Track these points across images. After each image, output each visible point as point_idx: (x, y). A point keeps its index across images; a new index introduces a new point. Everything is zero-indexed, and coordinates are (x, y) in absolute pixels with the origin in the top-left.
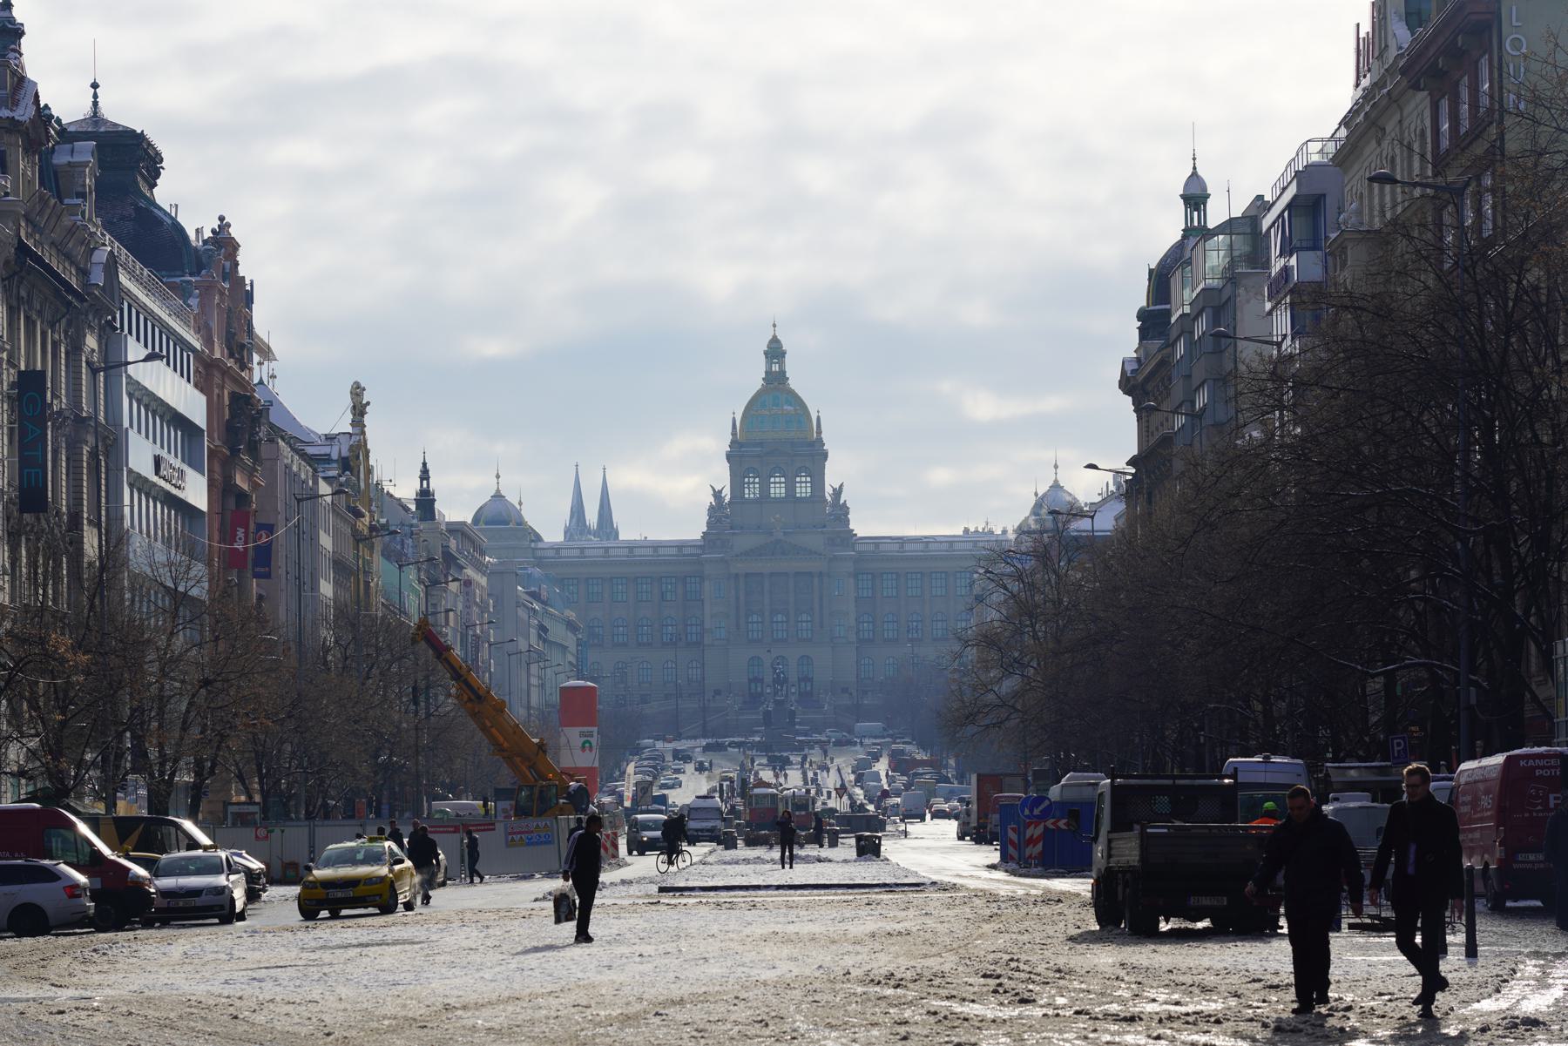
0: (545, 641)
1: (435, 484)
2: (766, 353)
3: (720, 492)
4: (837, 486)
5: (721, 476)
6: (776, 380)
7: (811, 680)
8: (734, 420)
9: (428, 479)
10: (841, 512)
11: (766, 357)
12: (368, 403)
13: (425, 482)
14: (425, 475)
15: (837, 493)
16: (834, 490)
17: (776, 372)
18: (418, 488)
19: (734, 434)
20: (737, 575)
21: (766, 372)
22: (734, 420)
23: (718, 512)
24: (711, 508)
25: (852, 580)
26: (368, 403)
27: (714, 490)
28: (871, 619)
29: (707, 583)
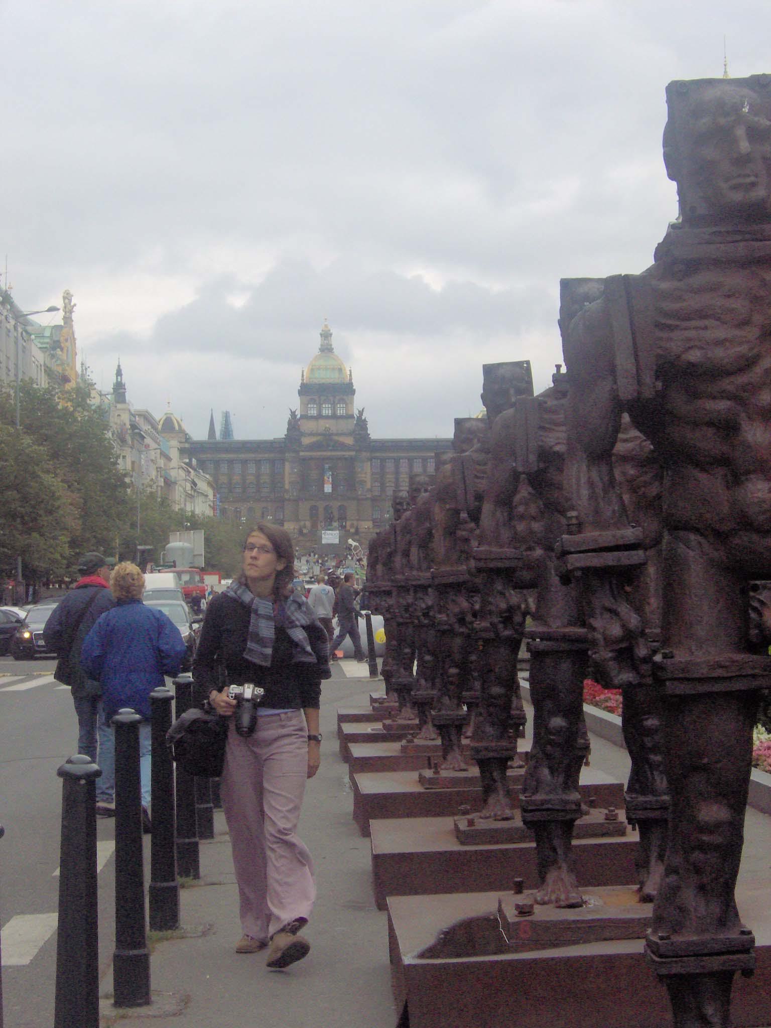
0: (195, 491)
1: (125, 379)
3: (295, 412)
5: (295, 403)
6: (327, 349)
8: (303, 371)
9: (121, 375)
10: (362, 424)
12: (75, 305)
13: (119, 378)
14: (119, 373)
15: (361, 413)
18: (115, 381)
19: (303, 380)
21: (321, 345)
22: (303, 371)
23: (294, 424)
24: (290, 423)
26: (75, 305)
27: (291, 410)
29: (287, 464)
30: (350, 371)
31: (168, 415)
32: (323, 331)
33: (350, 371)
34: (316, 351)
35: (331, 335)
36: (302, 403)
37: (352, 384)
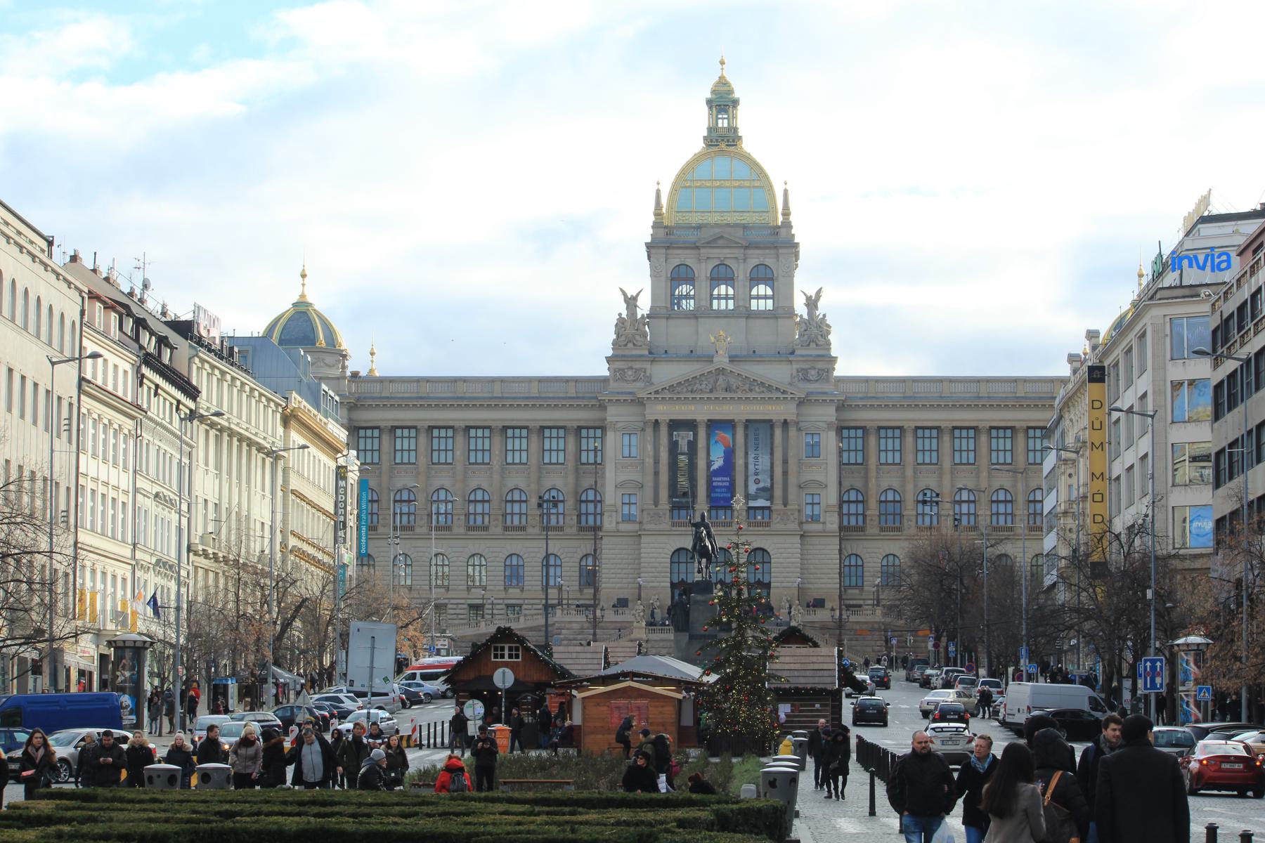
2: (709, 102)
3: (635, 299)
4: (812, 293)
7: (768, 586)
11: (710, 108)
15: (812, 303)
16: (809, 299)
17: (723, 128)
19: (658, 213)
20: (656, 423)
21: (710, 129)
23: (628, 331)
24: (621, 323)
25: (832, 435)
27: (624, 294)
28: (860, 498)
29: (610, 436)
30: (786, 192)
31: (302, 309)
32: (713, 92)
33: (786, 192)
34: (699, 146)
35: (735, 103)
36: (655, 275)
37: (787, 225)
